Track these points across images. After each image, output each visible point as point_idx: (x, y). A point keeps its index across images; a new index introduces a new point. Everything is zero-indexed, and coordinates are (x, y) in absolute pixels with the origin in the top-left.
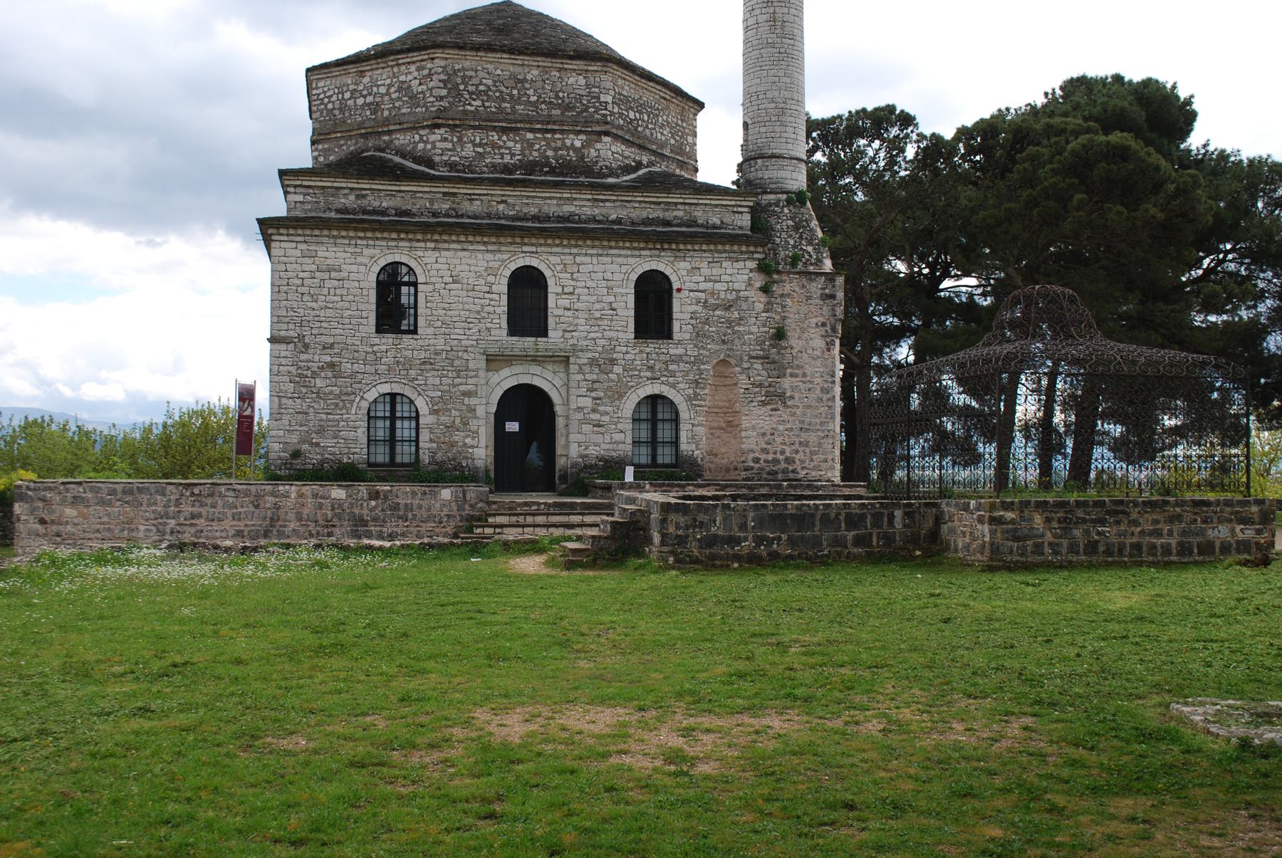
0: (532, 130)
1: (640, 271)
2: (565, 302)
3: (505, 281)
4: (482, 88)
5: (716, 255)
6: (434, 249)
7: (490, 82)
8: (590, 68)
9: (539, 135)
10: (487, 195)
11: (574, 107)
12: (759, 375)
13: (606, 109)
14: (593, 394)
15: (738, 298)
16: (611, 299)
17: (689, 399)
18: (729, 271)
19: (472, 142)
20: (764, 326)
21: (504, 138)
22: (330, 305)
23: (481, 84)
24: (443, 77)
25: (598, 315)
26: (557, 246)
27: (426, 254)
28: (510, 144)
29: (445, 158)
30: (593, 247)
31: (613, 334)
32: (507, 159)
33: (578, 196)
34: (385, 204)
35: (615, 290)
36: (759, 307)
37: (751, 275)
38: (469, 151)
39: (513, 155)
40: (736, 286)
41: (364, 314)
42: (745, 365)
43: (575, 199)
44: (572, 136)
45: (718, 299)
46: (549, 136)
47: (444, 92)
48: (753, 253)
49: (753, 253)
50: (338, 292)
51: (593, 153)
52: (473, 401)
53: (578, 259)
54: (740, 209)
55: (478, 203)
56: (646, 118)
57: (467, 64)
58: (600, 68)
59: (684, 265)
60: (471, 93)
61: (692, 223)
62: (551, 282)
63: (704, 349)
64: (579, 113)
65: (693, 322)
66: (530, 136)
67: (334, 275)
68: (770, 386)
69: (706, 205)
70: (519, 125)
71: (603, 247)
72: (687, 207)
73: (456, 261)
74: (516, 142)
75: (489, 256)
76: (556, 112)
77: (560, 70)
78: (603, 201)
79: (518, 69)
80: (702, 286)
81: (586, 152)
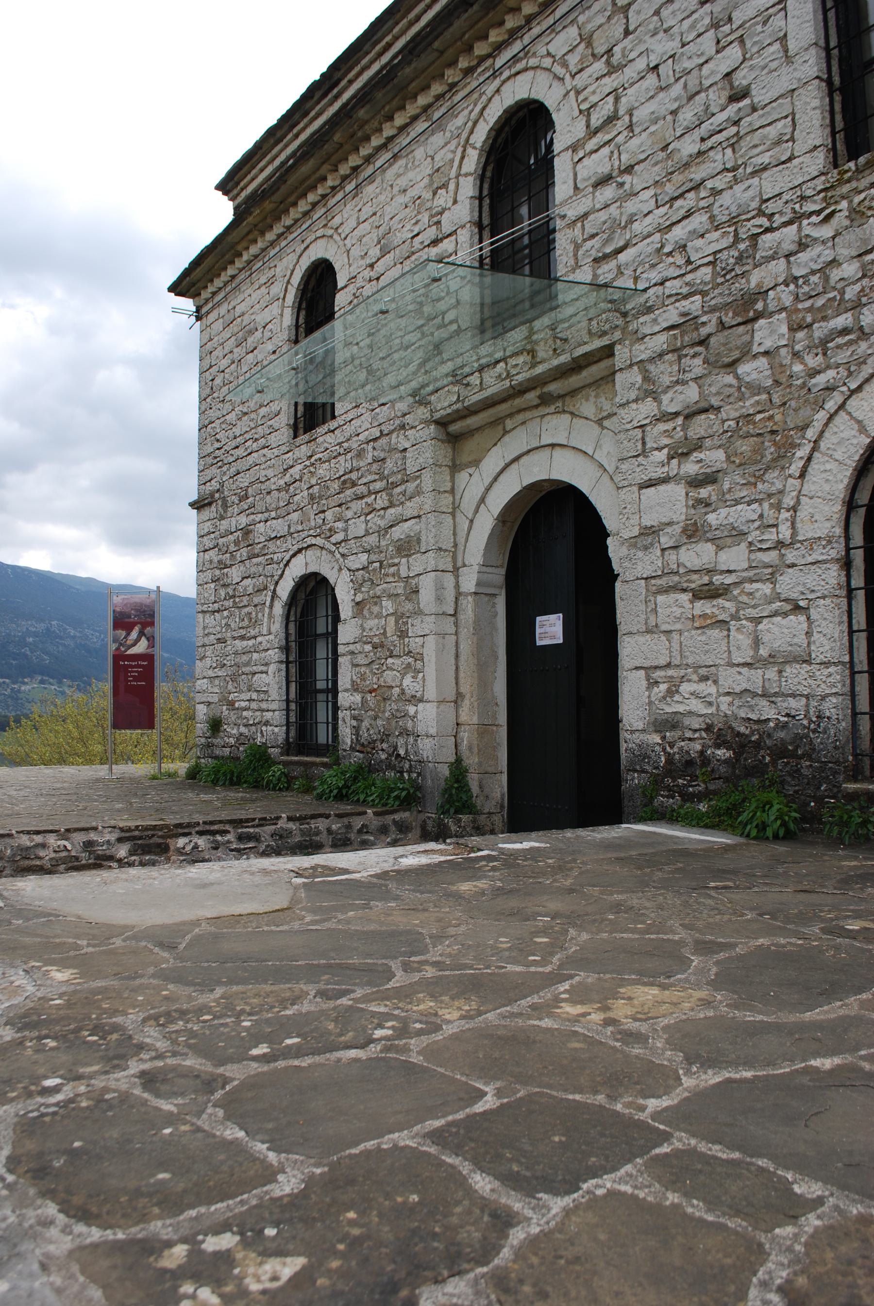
3: (468, 188)
14: (691, 468)
52: (418, 563)
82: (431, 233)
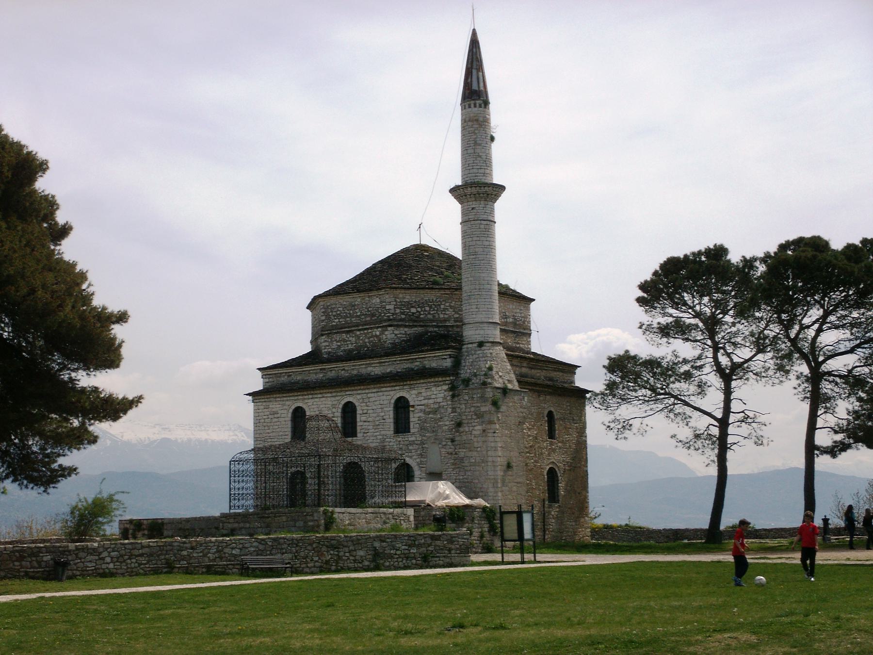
0: (359, 330)
1: (395, 398)
2: (363, 418)
3: (340, 410)
4: (338, 312)
5: (429, 385)
6: (312, 398)
7: (341, 309)
8: (380, 293)
9: (362, 332)
10: (337, 367)
11: (376, 315)
12: (450, 448)
13: (389, 313)
15: (440, 407)
16: (383, 414)
17: (418, 464)
18: (435, 393)
19: (336, 340)
20: (452, 421)
21: (348, 336)
22: (274, 430)
23: (338, 310)
24: (323, 310)
25: (377, 423)
26: (360, 390)
27: (309, 401)
28: (351, 339)
29: (326, 350)
30: (375, 388)
31: (383, 433)
32: (350, 347)
33: (373, 362)
34: (298, 379)
35: (385, 409)
36: (450, 410)
37: (445, 393)
38: (335, 345)
39: (352, 344)
40: (440, 400)
41: (287, 433)
42: (444, 443)
43: (372, 363)
44: (375, 330)
45: (430, 408)
46: (366, 331)
47: (323, 318)
48: (445, 381)
49: (445, 381)
50: (277, 423)
51: (384, 337)
53: (369, 395)
54: (446, 357)
55: (333, 372)
56: (427, 309)
57: (332, 302)
58: (383, 293)
59: (414, 392)
60: (335, 316)
61: (424, 368)
62: (358, 408)
63: (424, 436)
64: (378, 317)
65: (419, 422)
66: (358, 333)
67: (276, 416)
68: (456, 454)
69: (429, 357)
70: (353, 329)
71: (378, 388)
72: (421, 360)
73: (320, 403)
74: (353, 337)
75: (333, 399)
76: (368, 319)
77: (369, 297)
78: (384, 362)
79: (352, 300)
80: (423, 402)
81: (381, 336)
82: (332, 415)
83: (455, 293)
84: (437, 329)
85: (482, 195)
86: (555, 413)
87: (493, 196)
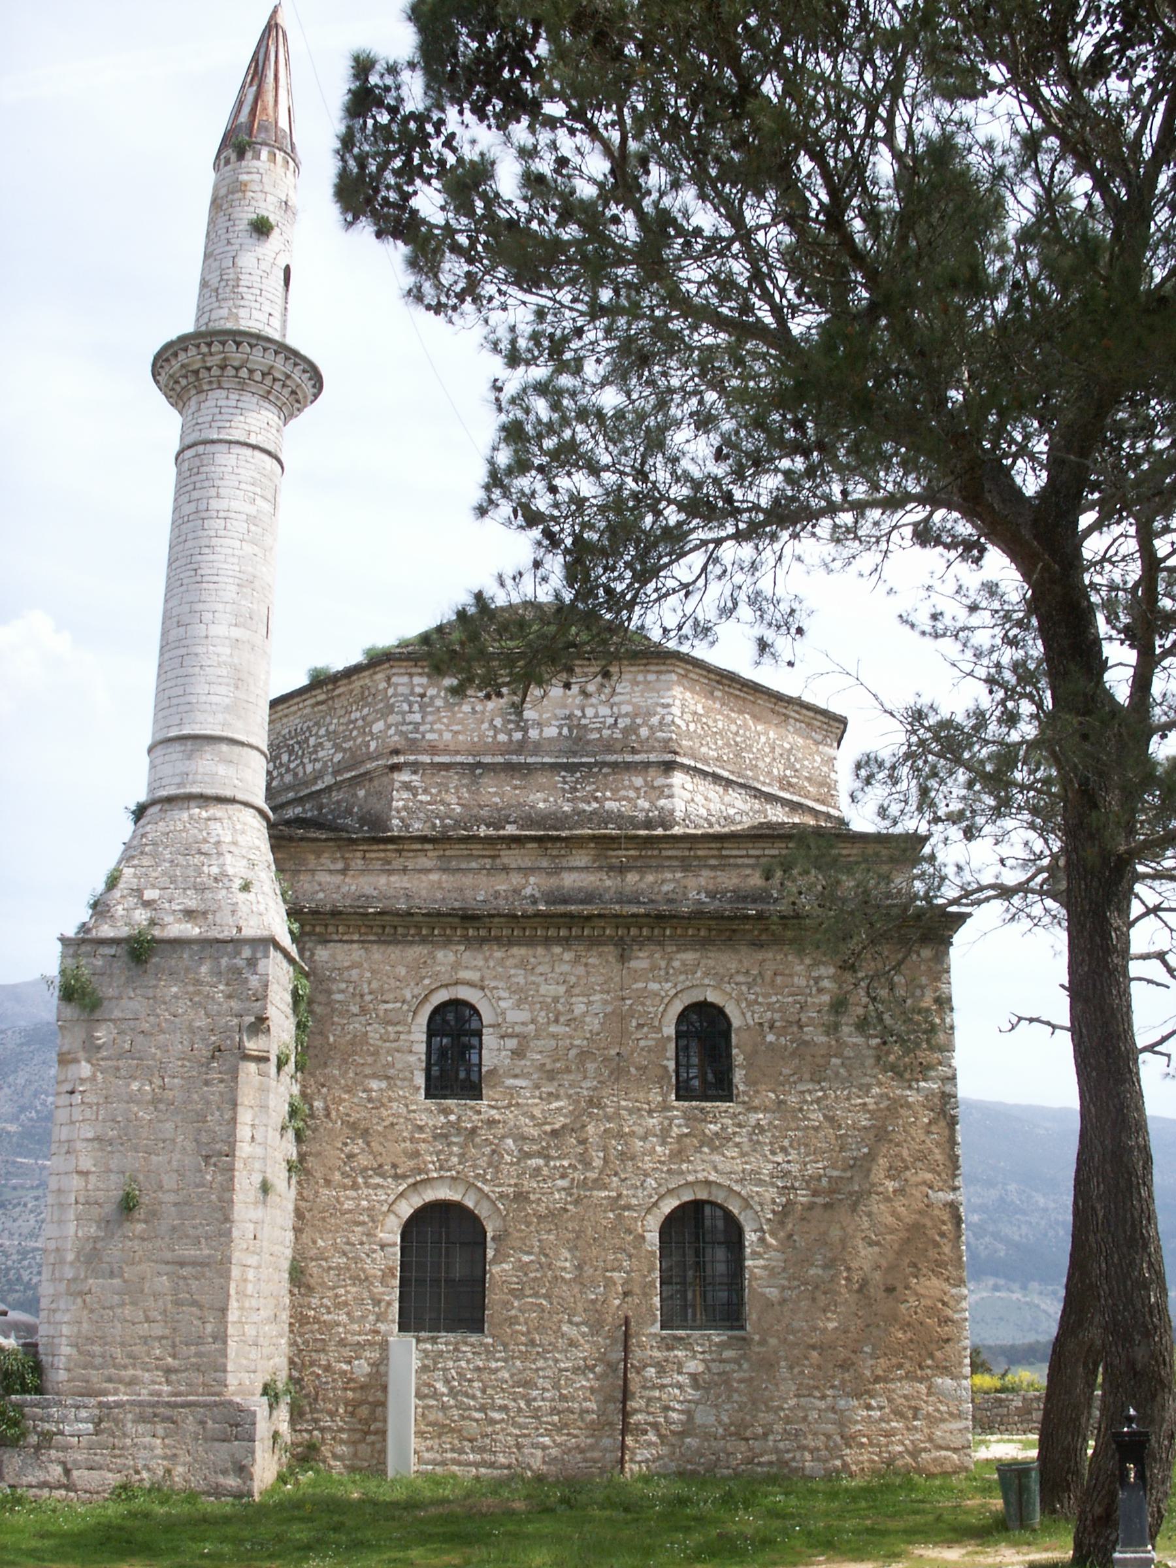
83: (337, 692)
84: (299, 810)
85: (184, 382)
86: (731, 1010)
87: (215, 371)
